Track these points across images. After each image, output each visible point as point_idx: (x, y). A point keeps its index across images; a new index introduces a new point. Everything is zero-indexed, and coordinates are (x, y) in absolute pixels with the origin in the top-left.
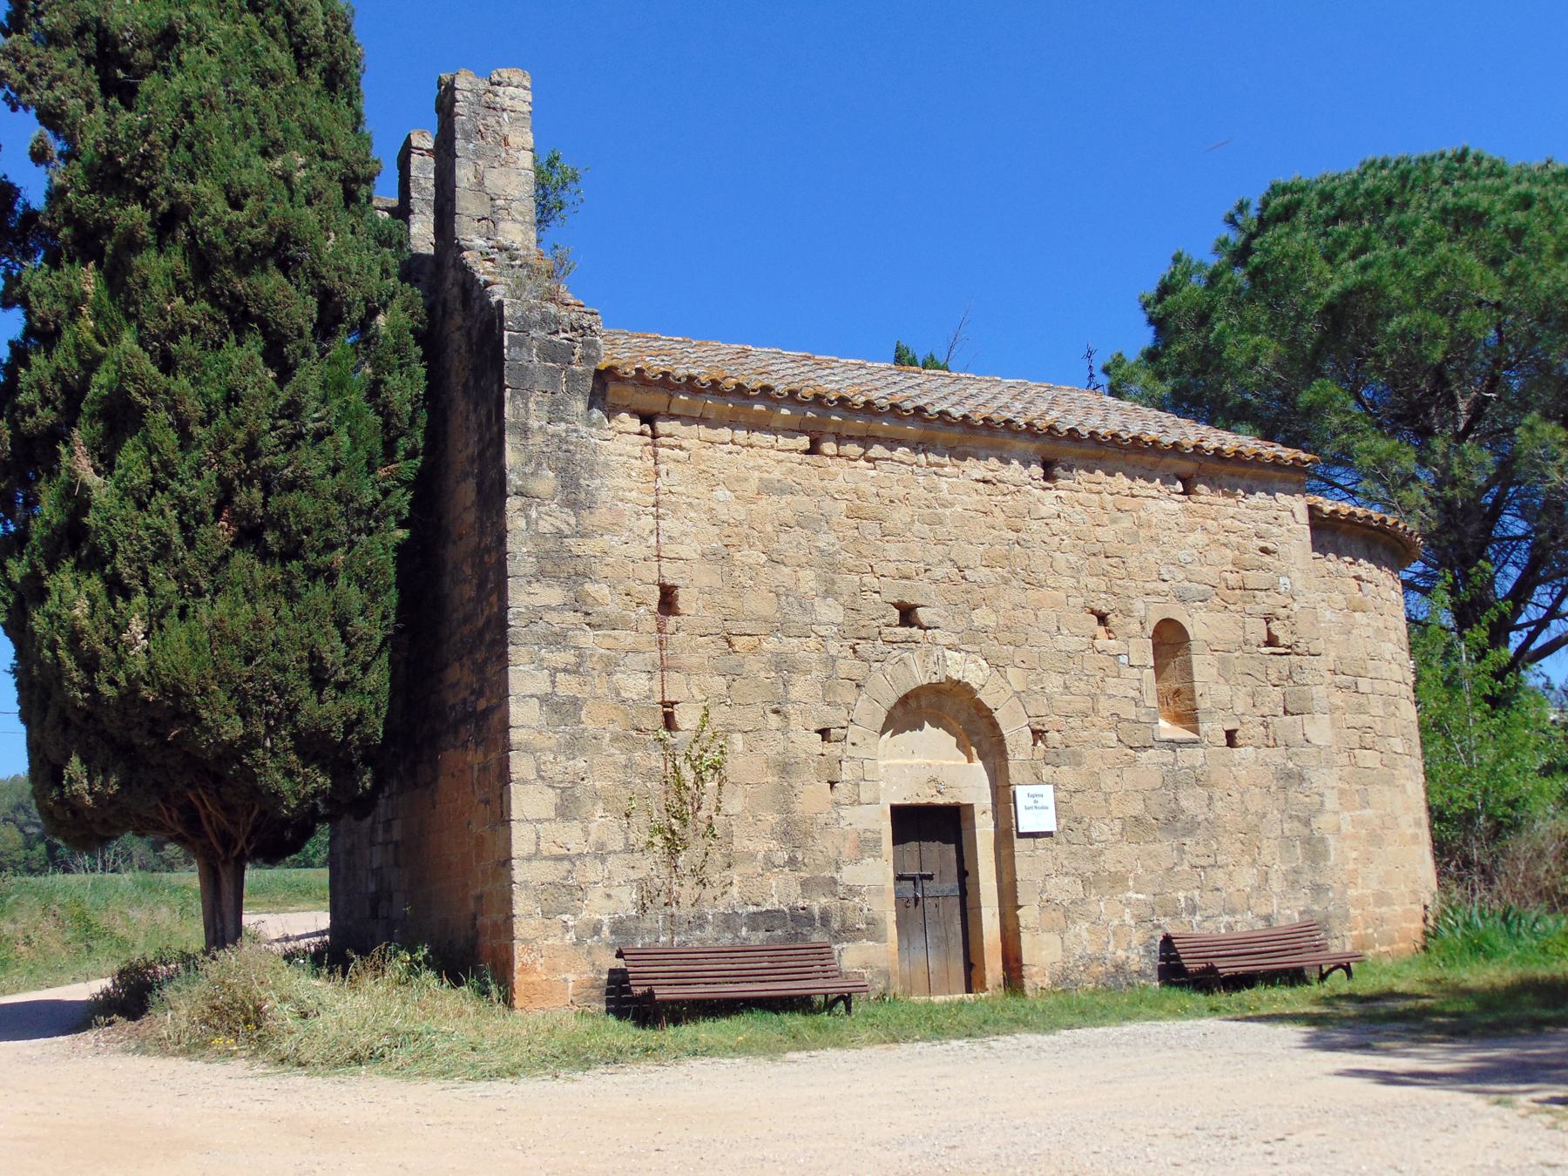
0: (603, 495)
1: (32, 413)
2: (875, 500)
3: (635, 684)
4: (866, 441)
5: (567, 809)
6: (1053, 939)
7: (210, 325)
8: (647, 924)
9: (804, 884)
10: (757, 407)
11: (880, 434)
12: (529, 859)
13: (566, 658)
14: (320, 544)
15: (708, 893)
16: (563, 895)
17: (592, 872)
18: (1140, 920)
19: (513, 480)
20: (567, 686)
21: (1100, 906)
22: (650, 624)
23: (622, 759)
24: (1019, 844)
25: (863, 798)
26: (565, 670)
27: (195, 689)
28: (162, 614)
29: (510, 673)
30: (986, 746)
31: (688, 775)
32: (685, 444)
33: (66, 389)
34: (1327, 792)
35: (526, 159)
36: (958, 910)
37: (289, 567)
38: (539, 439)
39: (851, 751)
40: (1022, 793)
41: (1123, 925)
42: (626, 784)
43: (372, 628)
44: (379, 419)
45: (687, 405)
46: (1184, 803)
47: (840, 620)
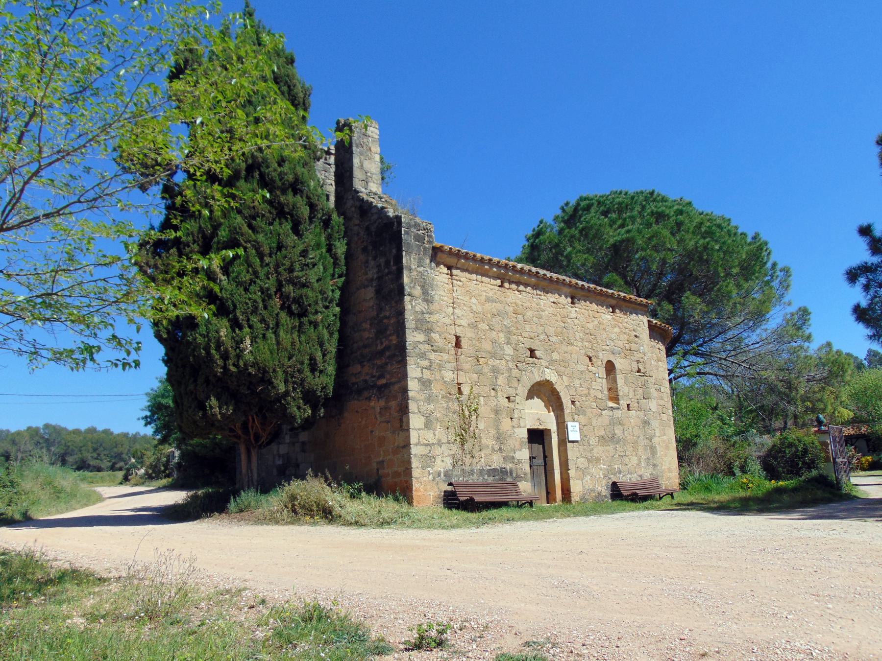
0: (436, 298)
1: (189, 246)
2: (521, 307)
3: (449, 375)
4: (518, 283)
5: (428, 425)
6: (579, 482)
7: (268, 215)
8: (455, 473)
9: (505, 458)
10: (486, 267)
11: (523, 281)
12: (416, 445)
13: (425, 363)
14: (313, 311)
15: (475, 461)
16: (429, 459)
17: (437, 451)
18: (605, 476)
19: (407, 289)
20: (427, 375)
21: (593, 470)
22: (453, 352)
23: (445, 405)
24: (569, 445)
25: (522, 425)
26: (426, 368)
27: (271, 370)
28: (256, 338)
29: (408, 369)
30: (554, 406)
31: (467, 413)
32: (462, 279)
33: (204, 237)
34: (656, 429)
35: (377, 158)
36: (543, 471)
37: (302, 320)
38: (415, 273)
39: (517, 406)
40: (570, 424)
41: (600, 477)
42: (447, 415)
43: (332, 347)
44: (332, 260)
45: (463, 264)
46: (616, 431)
47: (512, 354)
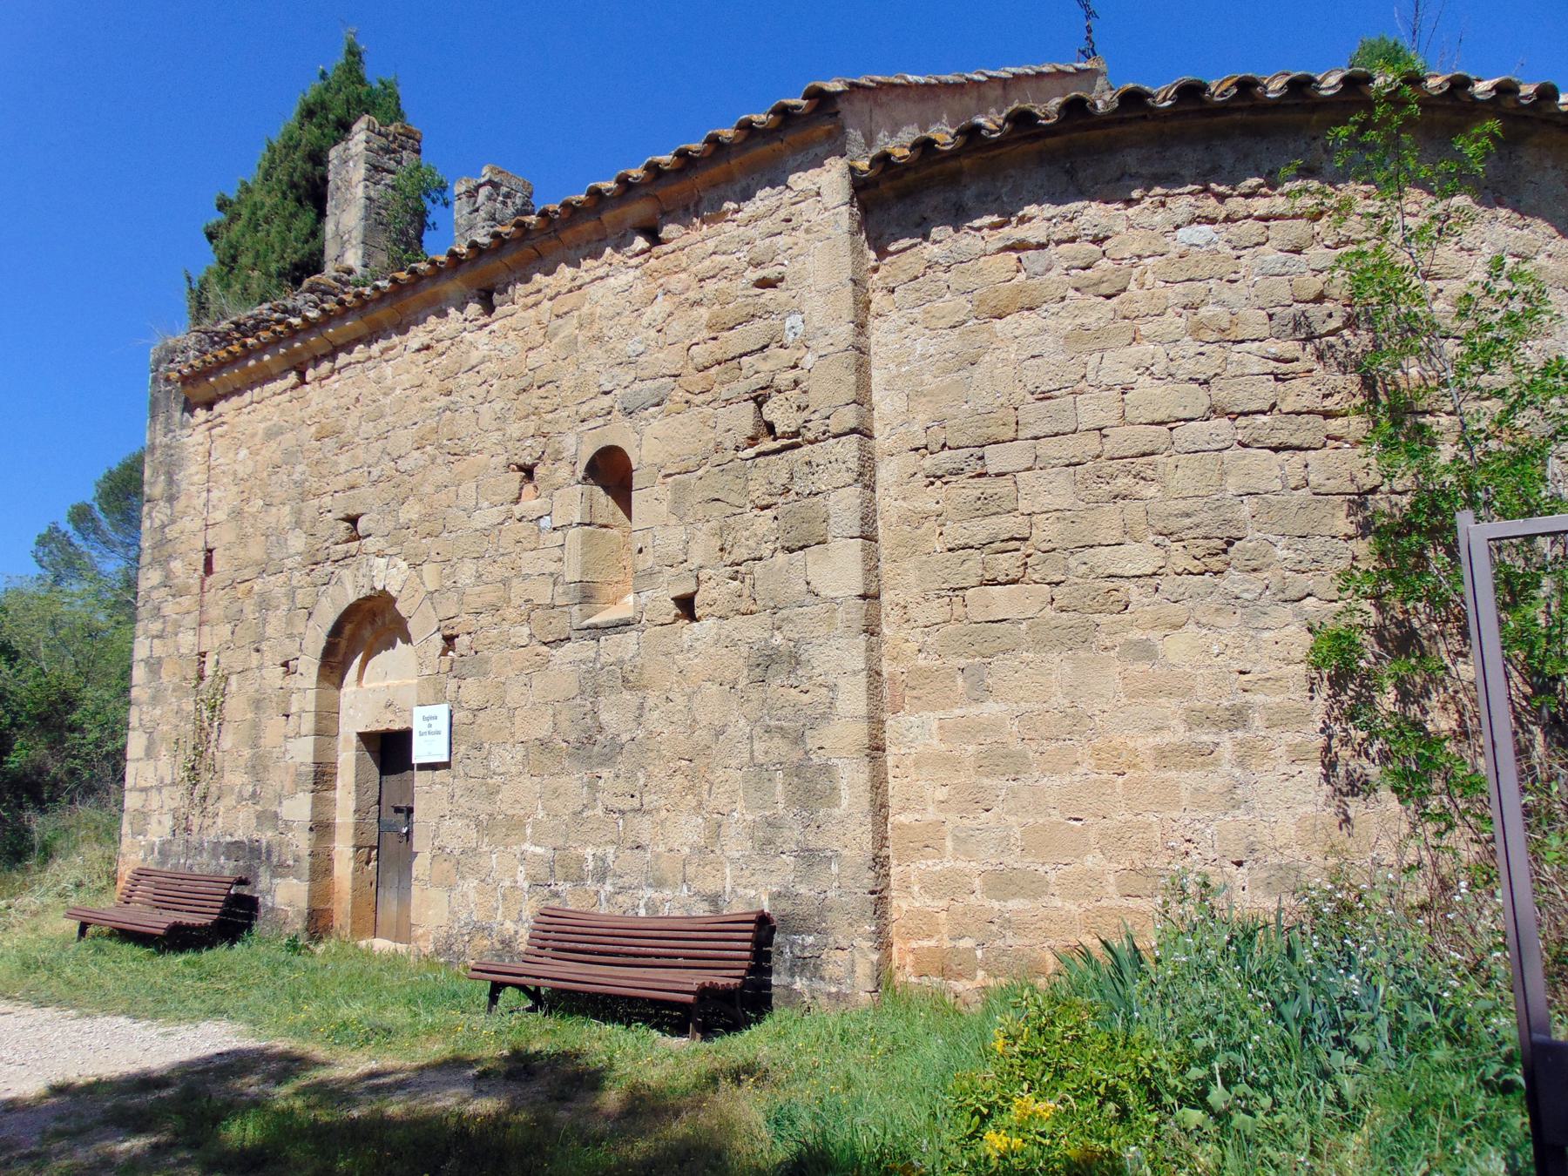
4: (332, 355)
15: (208, 822)
18: (536, 883)
34: (841, 682)
46: (604, 717)
